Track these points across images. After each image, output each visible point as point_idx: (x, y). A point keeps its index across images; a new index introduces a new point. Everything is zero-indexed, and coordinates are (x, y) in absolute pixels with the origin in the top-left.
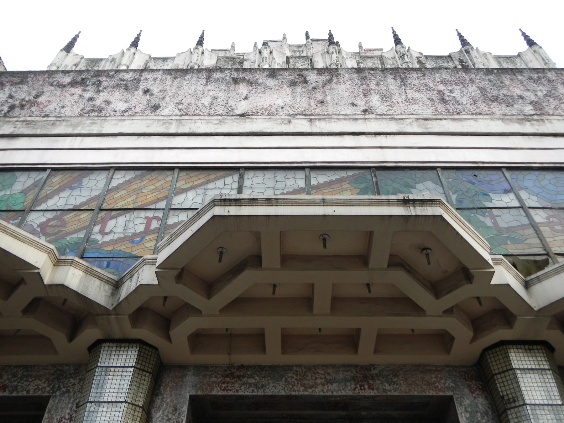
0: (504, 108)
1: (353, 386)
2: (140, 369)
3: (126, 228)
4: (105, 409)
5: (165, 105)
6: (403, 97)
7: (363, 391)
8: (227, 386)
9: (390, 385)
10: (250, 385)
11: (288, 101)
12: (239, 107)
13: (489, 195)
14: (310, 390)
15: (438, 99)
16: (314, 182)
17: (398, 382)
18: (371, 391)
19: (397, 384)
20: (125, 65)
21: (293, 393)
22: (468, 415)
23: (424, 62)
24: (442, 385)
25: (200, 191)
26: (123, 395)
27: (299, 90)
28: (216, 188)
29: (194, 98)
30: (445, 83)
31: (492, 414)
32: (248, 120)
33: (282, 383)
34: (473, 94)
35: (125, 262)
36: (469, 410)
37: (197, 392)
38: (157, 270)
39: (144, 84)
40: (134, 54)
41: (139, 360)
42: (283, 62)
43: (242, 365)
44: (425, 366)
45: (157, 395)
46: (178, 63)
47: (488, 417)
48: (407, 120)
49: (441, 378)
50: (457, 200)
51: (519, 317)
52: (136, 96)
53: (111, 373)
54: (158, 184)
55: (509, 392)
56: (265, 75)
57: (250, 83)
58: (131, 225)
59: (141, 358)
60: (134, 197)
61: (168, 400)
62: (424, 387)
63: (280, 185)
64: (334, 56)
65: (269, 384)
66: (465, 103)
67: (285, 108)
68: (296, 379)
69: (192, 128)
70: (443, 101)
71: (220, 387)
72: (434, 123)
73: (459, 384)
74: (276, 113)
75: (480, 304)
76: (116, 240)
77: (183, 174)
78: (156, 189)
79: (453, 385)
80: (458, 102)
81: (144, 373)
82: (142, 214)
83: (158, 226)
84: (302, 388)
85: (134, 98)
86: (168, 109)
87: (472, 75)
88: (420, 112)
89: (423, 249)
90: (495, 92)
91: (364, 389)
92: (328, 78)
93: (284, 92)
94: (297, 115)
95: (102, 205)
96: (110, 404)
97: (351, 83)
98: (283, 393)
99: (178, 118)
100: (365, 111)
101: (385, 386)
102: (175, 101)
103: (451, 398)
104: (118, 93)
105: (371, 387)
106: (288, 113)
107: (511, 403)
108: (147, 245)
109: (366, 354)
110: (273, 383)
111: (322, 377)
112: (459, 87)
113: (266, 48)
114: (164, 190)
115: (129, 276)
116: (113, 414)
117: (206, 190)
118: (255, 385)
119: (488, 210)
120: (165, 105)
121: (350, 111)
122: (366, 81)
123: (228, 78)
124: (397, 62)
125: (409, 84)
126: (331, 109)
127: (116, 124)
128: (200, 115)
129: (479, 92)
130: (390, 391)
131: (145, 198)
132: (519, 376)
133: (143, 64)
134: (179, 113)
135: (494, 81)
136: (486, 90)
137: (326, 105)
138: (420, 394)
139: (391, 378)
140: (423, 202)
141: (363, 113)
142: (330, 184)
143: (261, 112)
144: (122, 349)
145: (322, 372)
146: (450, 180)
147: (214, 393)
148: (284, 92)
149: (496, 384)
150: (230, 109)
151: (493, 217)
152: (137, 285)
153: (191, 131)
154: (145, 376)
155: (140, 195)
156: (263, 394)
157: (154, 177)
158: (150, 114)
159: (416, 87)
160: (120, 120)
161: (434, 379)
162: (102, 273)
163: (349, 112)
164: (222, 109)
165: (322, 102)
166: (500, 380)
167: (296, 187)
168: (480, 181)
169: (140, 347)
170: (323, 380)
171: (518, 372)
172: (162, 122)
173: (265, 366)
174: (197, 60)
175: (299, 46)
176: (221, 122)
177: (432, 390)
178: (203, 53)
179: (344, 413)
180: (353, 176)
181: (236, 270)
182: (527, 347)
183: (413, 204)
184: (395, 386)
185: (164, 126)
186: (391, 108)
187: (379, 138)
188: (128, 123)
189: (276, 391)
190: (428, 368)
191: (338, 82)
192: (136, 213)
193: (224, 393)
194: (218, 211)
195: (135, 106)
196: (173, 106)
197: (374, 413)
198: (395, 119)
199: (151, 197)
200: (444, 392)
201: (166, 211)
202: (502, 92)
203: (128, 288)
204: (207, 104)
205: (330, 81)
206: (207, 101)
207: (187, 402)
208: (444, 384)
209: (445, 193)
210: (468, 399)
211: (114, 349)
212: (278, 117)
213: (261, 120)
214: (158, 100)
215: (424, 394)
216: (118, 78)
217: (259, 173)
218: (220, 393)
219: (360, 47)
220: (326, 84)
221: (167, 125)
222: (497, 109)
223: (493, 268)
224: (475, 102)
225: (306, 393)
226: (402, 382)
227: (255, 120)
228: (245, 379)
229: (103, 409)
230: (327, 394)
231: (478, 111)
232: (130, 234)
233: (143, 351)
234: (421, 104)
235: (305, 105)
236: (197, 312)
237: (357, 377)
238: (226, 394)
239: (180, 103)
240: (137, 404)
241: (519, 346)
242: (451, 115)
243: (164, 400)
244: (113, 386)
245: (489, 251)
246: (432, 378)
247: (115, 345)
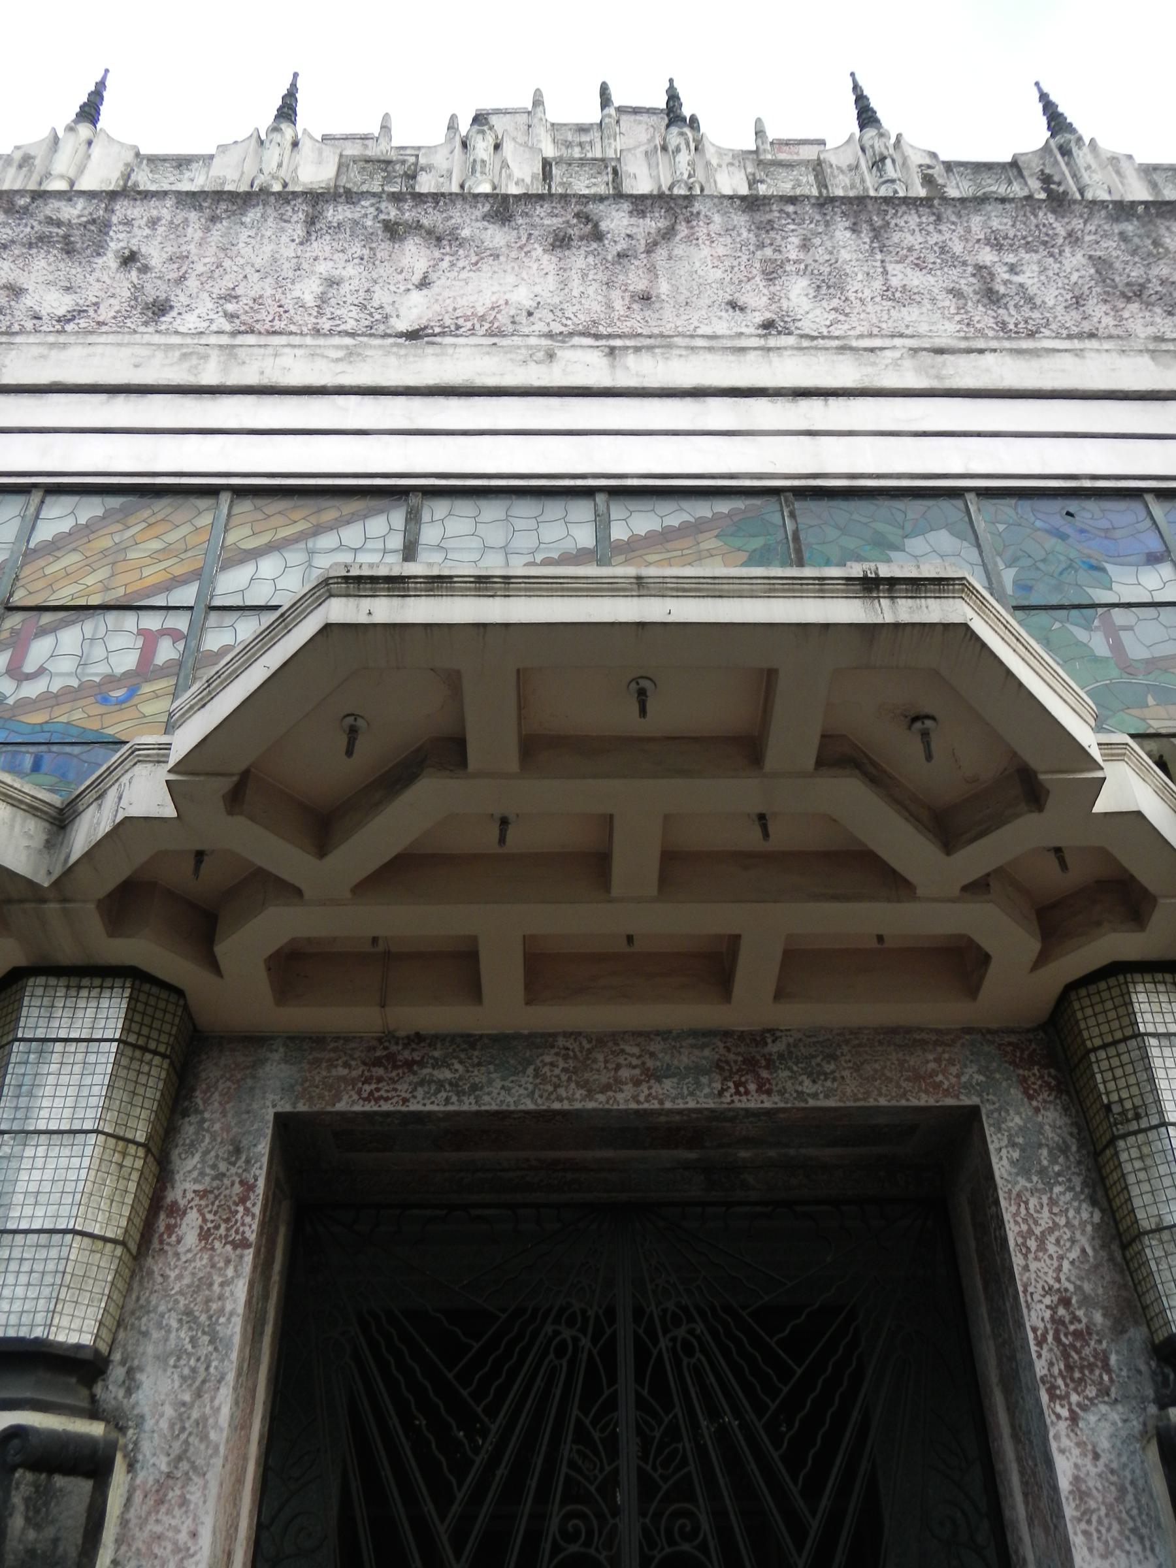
0: (1158, 320)
1: (718, 1086)
2: (135, 1046)
3: (83, 662)
4: (41, 1151)
5: (183, 299)
6: (878, 284)
7: (744, 1098)
8: (378, 1090)
9: (814, 1082)
10: (441, 1085)
11: (546, 294)
12: (403, 311)
13: (1104, 570)
14: (601, 1098)
15: (976, 293)
16: (619, 532)
17: (837, 1074)
18: (764, 1097)
19: (834, 1080)
20: (62, 177)
21: (557, 1106)
22: (1016, 1155)
23: (940, 181)
24: (954, 1080)
25: (295, 556)
26: (91, 1113)
27: (578, 259)
28: (341, 547)
29: (269, 280)
30: (996, 243)
31: (1078, 1151)
32: (430, 350)
33: (527, 1079)
34: (1074, 277)
35: (84, 757)
36: (1020, 1140)
37: (294, 1105)
38: (172, 777)
39: (121, 236)
40: (90, 143)
41: (132, 1021)
42: (534, 177)
43: (417, 1034)
44: (908, 1030)
45: (185, 1114)
46: (221, 174)
47: (1067, 1158)
48: (887, 353)
49: (951, 1062)
50: (1015, 583)
51: (1161, 901)
52: (96, 274)
53: (56, 1058)
54: (172, 537)
55: (1124, 1094)
56: (478, 213)
57: (435, 238)
58: (98, 652)
59: (138, 1018)
60: (103, 573)
61: (217, 1126)
62: (904, 1084)
63: (525, 541)
64: (683, 158)
65: (490, 1082)
66: (1050, 303)
67: (537, 315)
68: (564, 1070)
69: (268, 372)
70: (991, 297)
71: (359, 1092)
72: (963, 361)
73: (998, 1076)
74: (511, 328)
75: (1064, 866)
76: (56, 696)
77: (245, 505)
78: (166, 551)
79: (982, 1078)
80: (1030, 300)
81: (148, 1056)
82: (130, 621)
83: (174, 655)
84: (580, 1093)
85: (91, 279)
86: (196, 312)
87: (1075, 221)
88: (923, 328)
89: (915, 719)
90: (1136, 273)
91: (747, 1093)
92: (662, 224)
93: (535, 266)
94: (571, 334)
95: (11, 595)
96: (54, 1136)
97: (729, 240)
98: (530, 1106)
99: (225, 340)
100: (768, 325)
101: (801, 1083)
102: (216, 291)
103: (975, 1111)
104: (43, 263)
105: (764, 1088)
106: (546, 329)
107: (1128, 1121)
108: (148, 709)
109: (752, 1003)
110: (503, 1079)
111: (635, 1062)
112: (1035, 257)
113: (483, 132)
114: (189, 554)
115: (94, 795)
116: (63, 1162)
117: (311, 553)
118: (454, 1084)
119: (1100, 610)
120: (186, 301)
121: (723, 323)
122: (772, 234)
123: (369, 223)
124: (863, 181)
125: (897, 245)
126: (669, 320)
127: (43, 357)
128: (291, 333)
129: (1092, 271)
130: (815, 1096)
131: (135, 575)
132: (1155, 1052)
133: (117, 174)
134: (228, 327)
135: (1136, 240)
136: (1111, 266)
137: (657, 305)
138: (894, 1103)
139: (818, 1065)
140: (917, 586)
141: (760, 331)
142: (662, 538)
143: (469, 325)
144: (84, 993)
145: (636, 1050)
146: (1001, 527)
147: (341, 1106)
148: (535, 266)
149: (1093, 1075)
150: (378, 317)
151: (1112, 632)
152: (118, 821)
153: (265, 381)
154: (150, 1063)
155: (121, 567)
156: (474, 1108)
157: (160, 516)
158: (142, 329)
159: (915, 254)
160: (52, 345)
161: (932, 1065)
162: (16, 785)
163: (721, 328)
164: (354, 314)
165: (645, 298)
166: (1105, 1065)
167: (568, 546)
168: (1082, 531)
169: (132, 988)
170: (637, 1071)
171: (1153, 1041)
172: (177, 354)
173: (481, 1036)
174: (280, 165)
175: (582, 129)
176: (351, 355)
177: (926, 1092)
178: (295, 144)
179: (692, 1155)
180: (729, 515)
181: (397, 777)
183: (890, 590)
184: (828, 1083)
185: (186, 365)
186: (842, 318)
187: (804, 404)
188: (76, 353)
189: (509, 1099)
191: (691, 239)
192: (111, 617)
193: (370, 1107)
194: (341, 610)
195: (96, 304)
196: (210, 305)
197: (772, 1153)
198: (851, 349)
199: (153, 574)
200: (957, 1097)
201: (199, 612)
202: (1155, 271)
203: (92, 826)
204: (309, 300)
205: (668, 234)
206: (308, 290)
207: (269, 1132)
208: (958, 1076)
209: (984, 565)
210: (1019, 1113)
211: (61, 992)
212: (517, 340)
213: (468, 350)
214: (164, 287)
215: (903, 1103)
216: (41, 217)
217: (465, 507)
218: (357, 1108)
219: (759, 133)
220: (655, 244)
221: (194, 361)
222: (1141, 322)
223: (1102, 769)
224: (1078, 301)
225: (591, 1105)
226: (846, 1073)
227: (450, 351)
228: (426, 1071)
229: (36, 1151)
230: (646, 1106)
231: (1086, 327)
232: (97, 679)
234: (927, 304)
235: (596, 307)
236: (291, 892)
237: (727, 1062)
238: (376, 1108)
239: (231, 296)
240: (129, 1136)
241: (1159, 977)
242: (1010, 338)
243: (206, 1125)
244: (61, 1091)
245: (1093, 723)
246: (928, 1062)
247: (63, 981)
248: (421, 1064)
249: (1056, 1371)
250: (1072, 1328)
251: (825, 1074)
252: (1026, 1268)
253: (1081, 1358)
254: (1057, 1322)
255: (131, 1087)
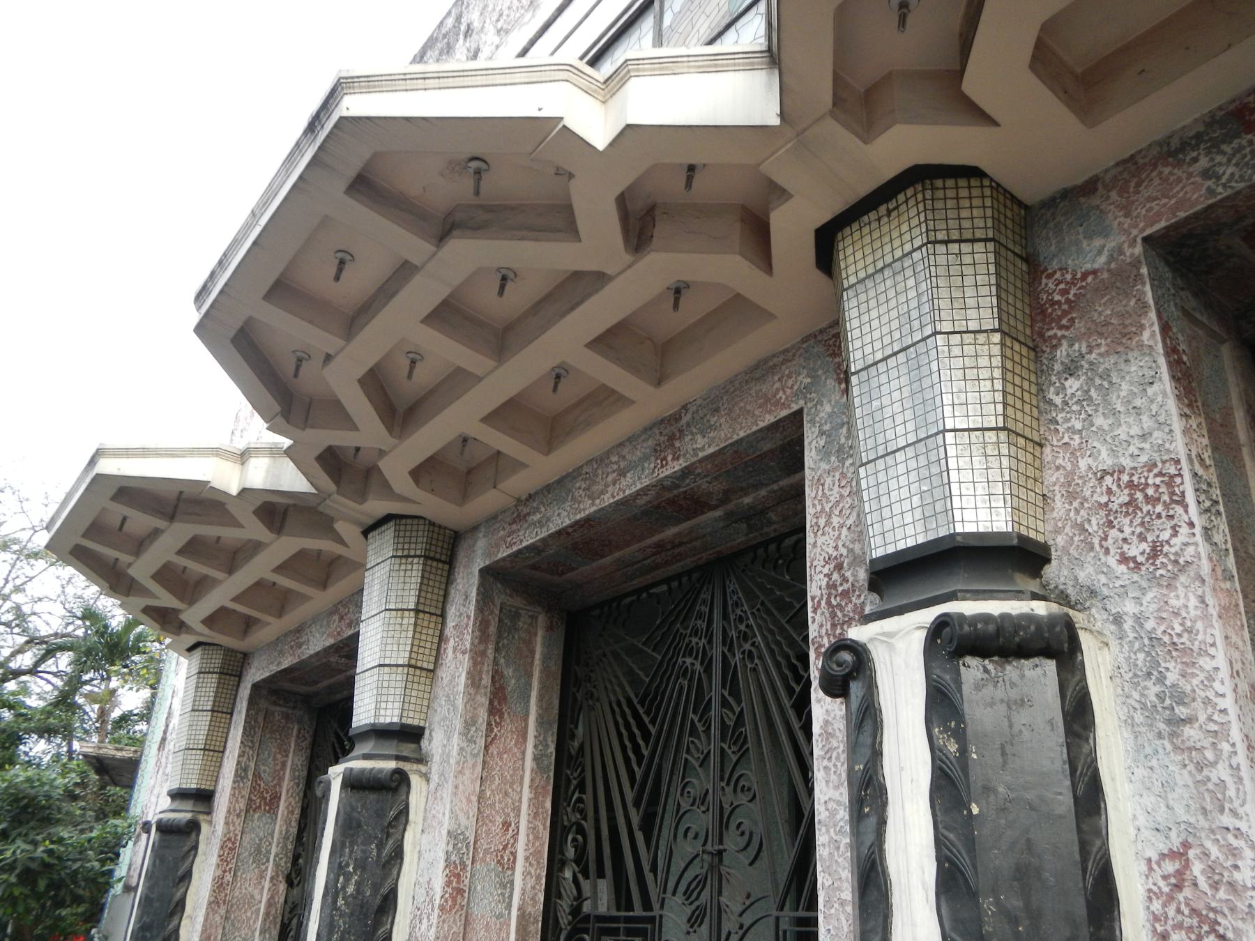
1: (652, 466)
21: (578, 517)
24: (789, 391)
36: (827, 427)
44: (766, 361)
49: (789, 377)
59: (401, 540)
79: (809, 380)
118: (540, 522)
130: (702, 449)
138: (749, 432)
147: (500, 556)
154: (412, 564)
177: (770, 412)
182: (883, 209)
190: (771, 364)
197: (763, 492)
215: (755, 428)
233: (402, 528)
240: (405, 607)
248: (529, 514)
249: (824, 631)
250: (840, 589)
251: (711, 426)
252: (815, 545)
253: (844, 616)
254: (831, 586)
255: (402, 580)
